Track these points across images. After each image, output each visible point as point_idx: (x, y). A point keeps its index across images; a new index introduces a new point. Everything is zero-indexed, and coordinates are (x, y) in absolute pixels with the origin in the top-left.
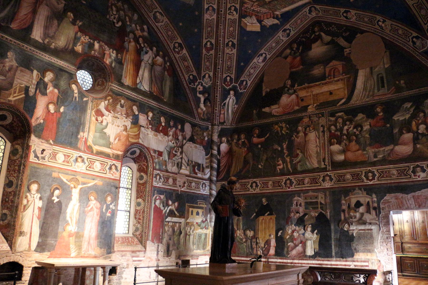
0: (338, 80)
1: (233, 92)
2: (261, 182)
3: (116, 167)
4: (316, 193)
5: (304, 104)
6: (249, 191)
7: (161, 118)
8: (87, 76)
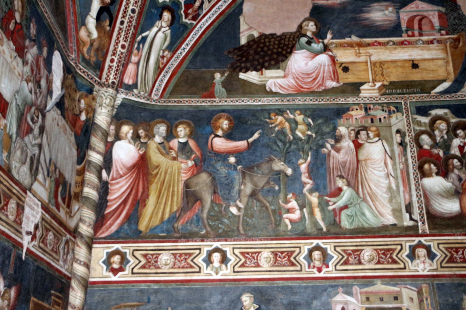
0: (431, 42)
1: (170, 17)
4: (394, 285)
5: (350, 78)
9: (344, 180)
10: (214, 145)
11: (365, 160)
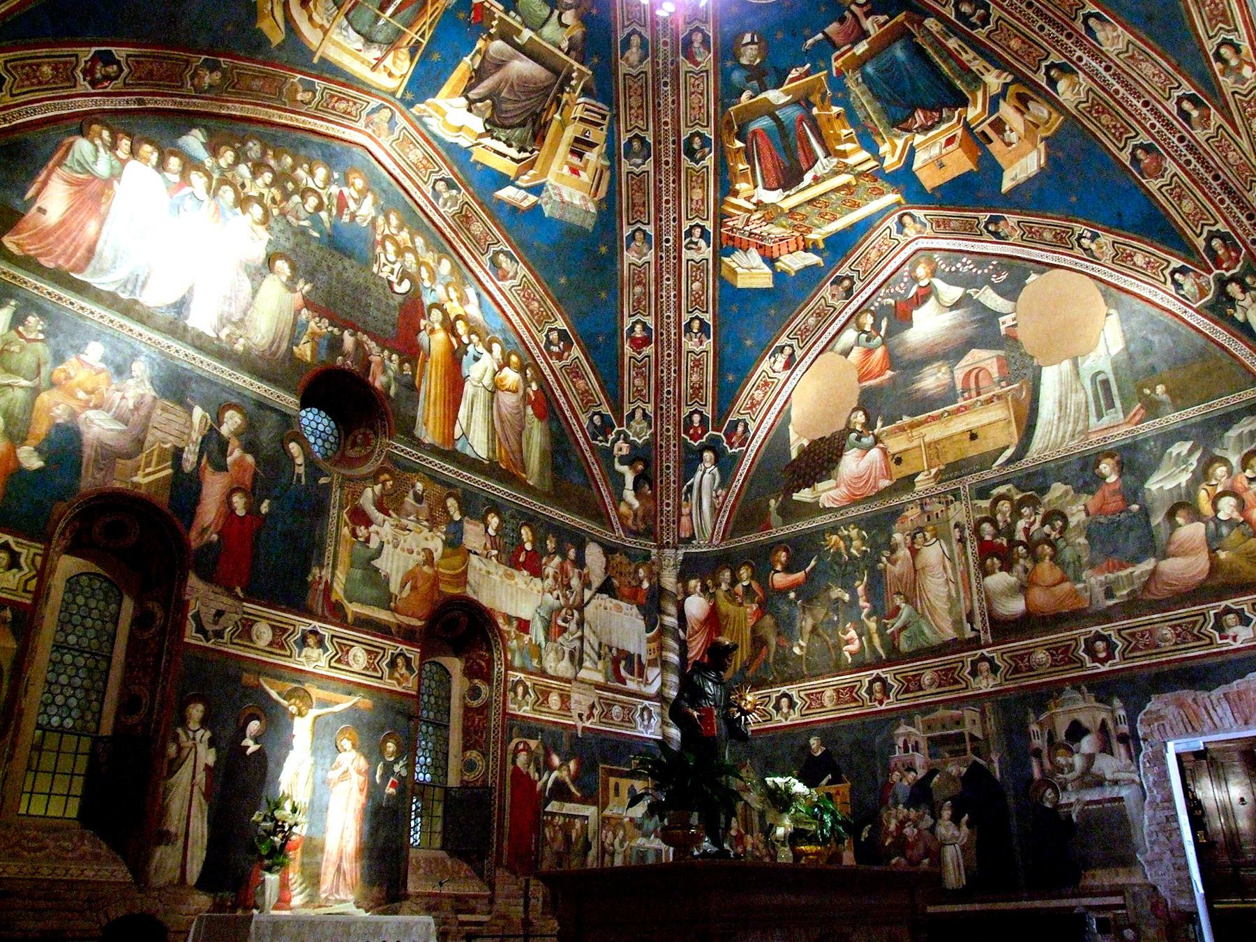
0: (990, 401)
2: (802, 694)
3: (408, 662)
5: (904, 470)
7: (523, 531)
8: (326, 422)
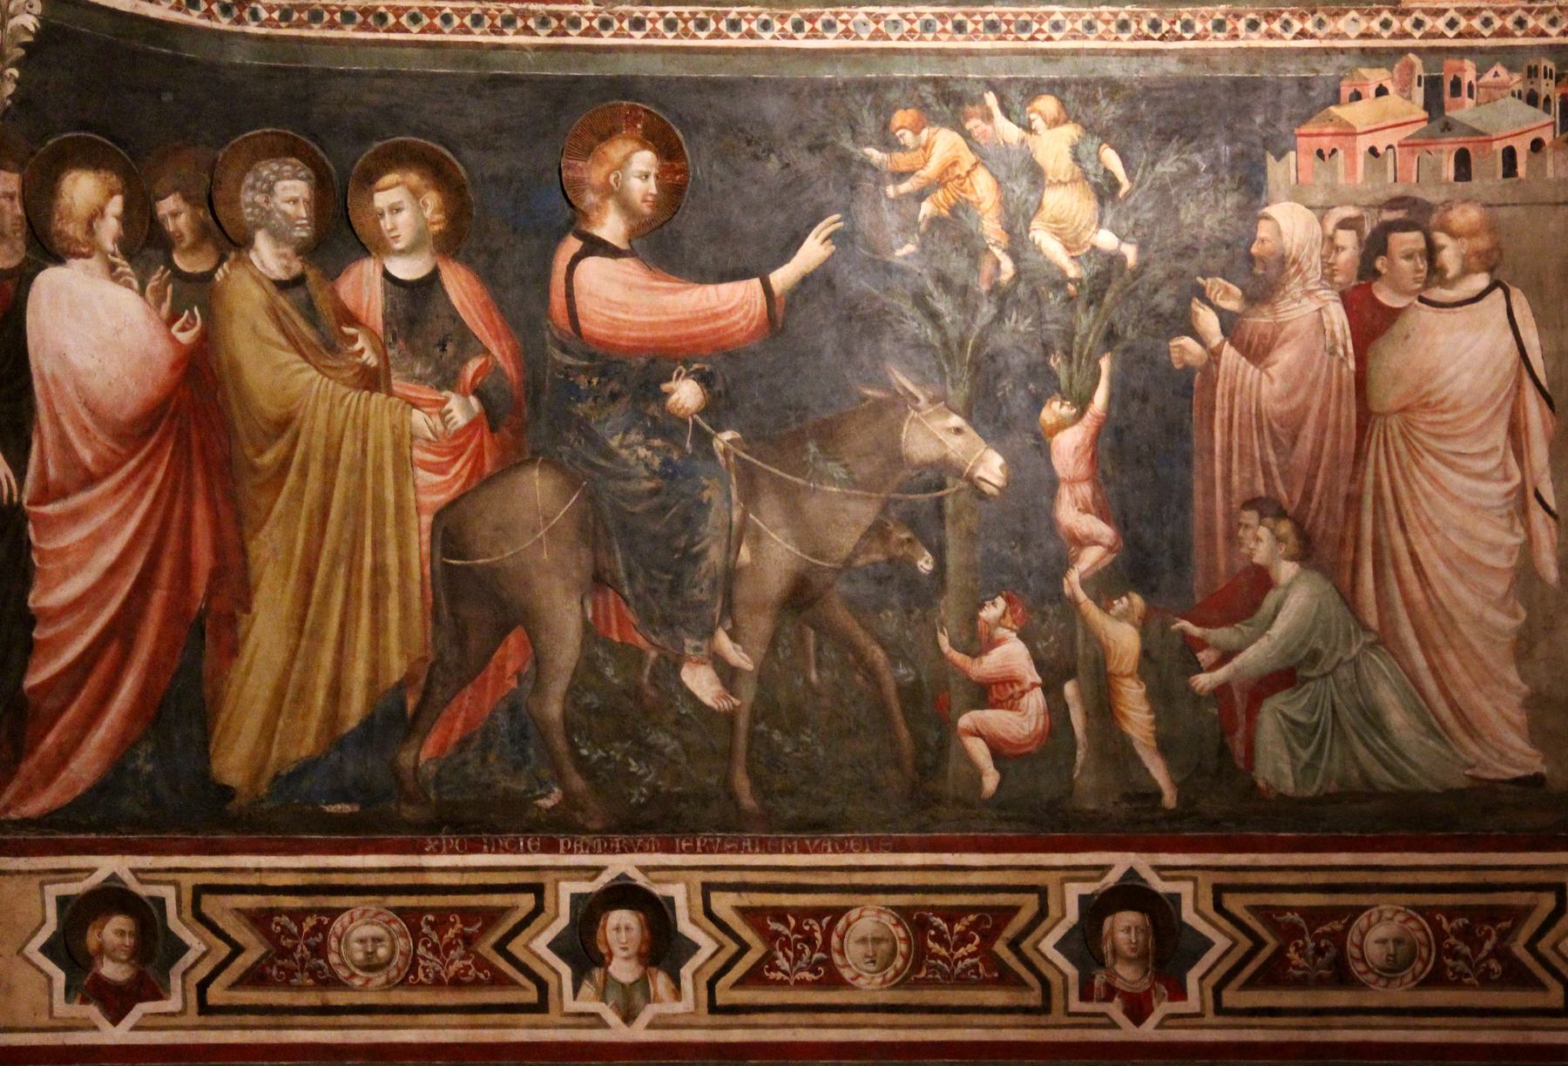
2: (723, 904)
6: (541, 1007)
9: (1285, 528)
10: (587, 305)
11: (1404, 410)
